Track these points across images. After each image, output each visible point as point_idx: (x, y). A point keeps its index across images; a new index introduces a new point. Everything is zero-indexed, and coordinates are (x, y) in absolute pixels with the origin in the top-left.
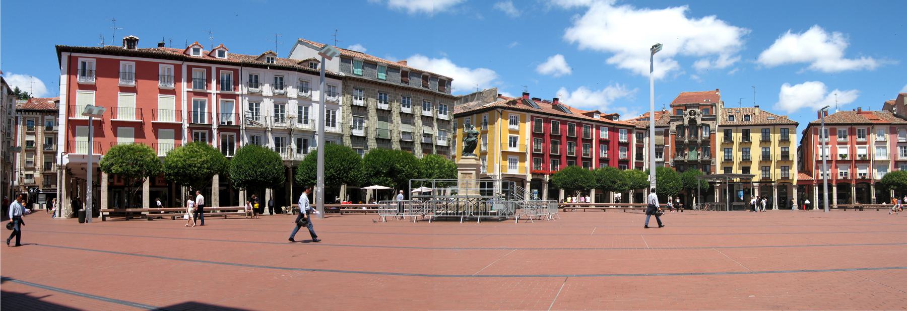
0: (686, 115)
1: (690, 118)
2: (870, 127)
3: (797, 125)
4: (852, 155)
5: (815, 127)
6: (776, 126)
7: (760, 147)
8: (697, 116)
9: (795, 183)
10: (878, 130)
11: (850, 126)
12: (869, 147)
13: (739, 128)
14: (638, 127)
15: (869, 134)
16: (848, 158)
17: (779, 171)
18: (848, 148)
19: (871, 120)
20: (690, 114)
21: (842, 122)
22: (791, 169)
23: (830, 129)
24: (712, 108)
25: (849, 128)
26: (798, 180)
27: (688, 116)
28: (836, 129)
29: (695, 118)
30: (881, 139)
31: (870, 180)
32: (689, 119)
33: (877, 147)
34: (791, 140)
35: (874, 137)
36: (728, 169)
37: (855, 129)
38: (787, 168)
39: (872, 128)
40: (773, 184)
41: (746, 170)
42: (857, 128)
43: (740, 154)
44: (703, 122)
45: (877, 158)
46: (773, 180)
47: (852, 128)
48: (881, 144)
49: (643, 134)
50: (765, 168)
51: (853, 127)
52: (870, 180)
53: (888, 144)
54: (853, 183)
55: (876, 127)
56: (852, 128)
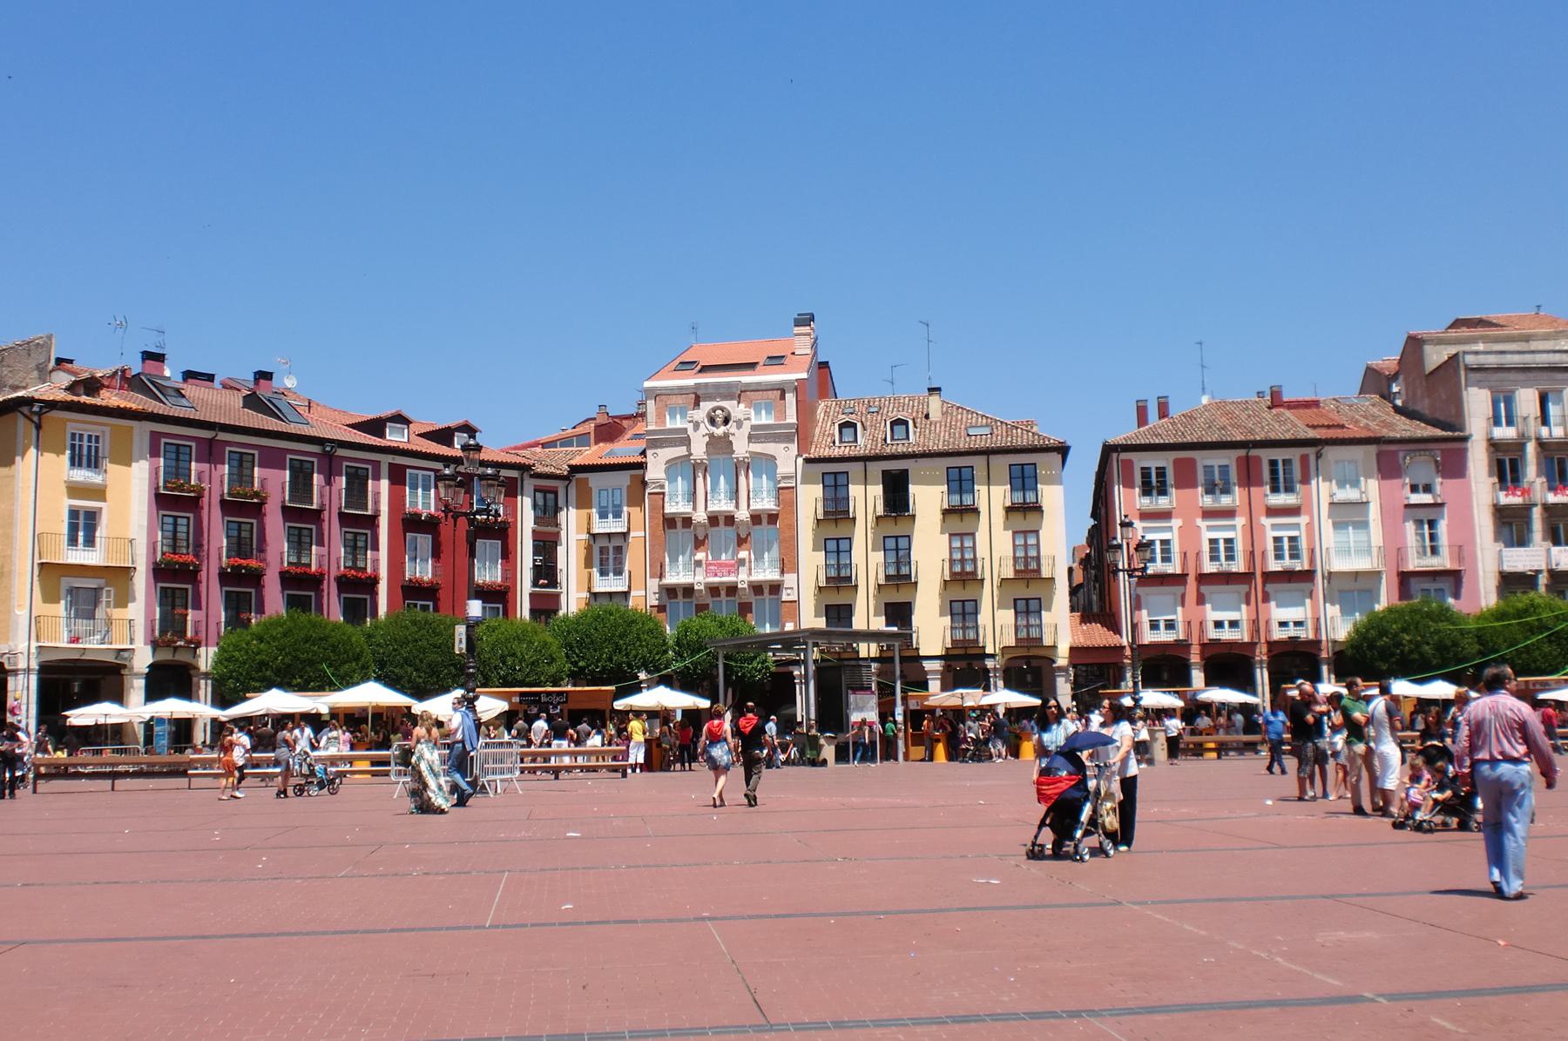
0: (697, 426)
1: (711, 436)
2: (1311, 451)
3: (1063, 450)
4: (1252, 553)
5: (1124, 456)
6: (991, 457)
7: (942, 533)
8: (732, 427)
9: (1062, 660)
10: (1337, 462)
11: (1242, 452)
12: (1310, 526)
13: (871, 466)
14: (540, 469)
15: (1306, 480)
16: (1239, 566)
17: (1007, 617)
18: (1239, 528)
19: (1314, 427)
20: (712, 421)
21: (1214, 438)
22: (1049, 609)
23: (1177, 462)
24: (783, 397)
25: (1239, 459)
26: (1071, 649)
27: (705, 428)
28: (1192, 462)
29: (726, 435)
30: (1350, 494)
31: (1316, 643)
32: (707, 439)
33: (1337, 525)
34: (1046, 504)
35: (1323, 491)
36: (839, 614)
37: (1258, 460)
38: (1033, 605)
39: (1318, 456)
40: (990, 664)
41: (899, 613)
42: (1266, 455)
43: (878, 557)
44: (757, 448)
45: (1339, 565)
46: (989, 650)
47: (1247, 457)
48: (1349, 514)
49: (556, 493)
50: (962, 610)
51: (1254, 452)
52: (1316, 643)
53: (1374, 513)
54: (1261, 654)
55: (1331, 453)
56: (1247, 457)
